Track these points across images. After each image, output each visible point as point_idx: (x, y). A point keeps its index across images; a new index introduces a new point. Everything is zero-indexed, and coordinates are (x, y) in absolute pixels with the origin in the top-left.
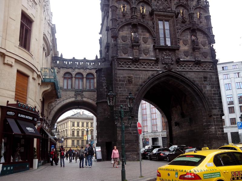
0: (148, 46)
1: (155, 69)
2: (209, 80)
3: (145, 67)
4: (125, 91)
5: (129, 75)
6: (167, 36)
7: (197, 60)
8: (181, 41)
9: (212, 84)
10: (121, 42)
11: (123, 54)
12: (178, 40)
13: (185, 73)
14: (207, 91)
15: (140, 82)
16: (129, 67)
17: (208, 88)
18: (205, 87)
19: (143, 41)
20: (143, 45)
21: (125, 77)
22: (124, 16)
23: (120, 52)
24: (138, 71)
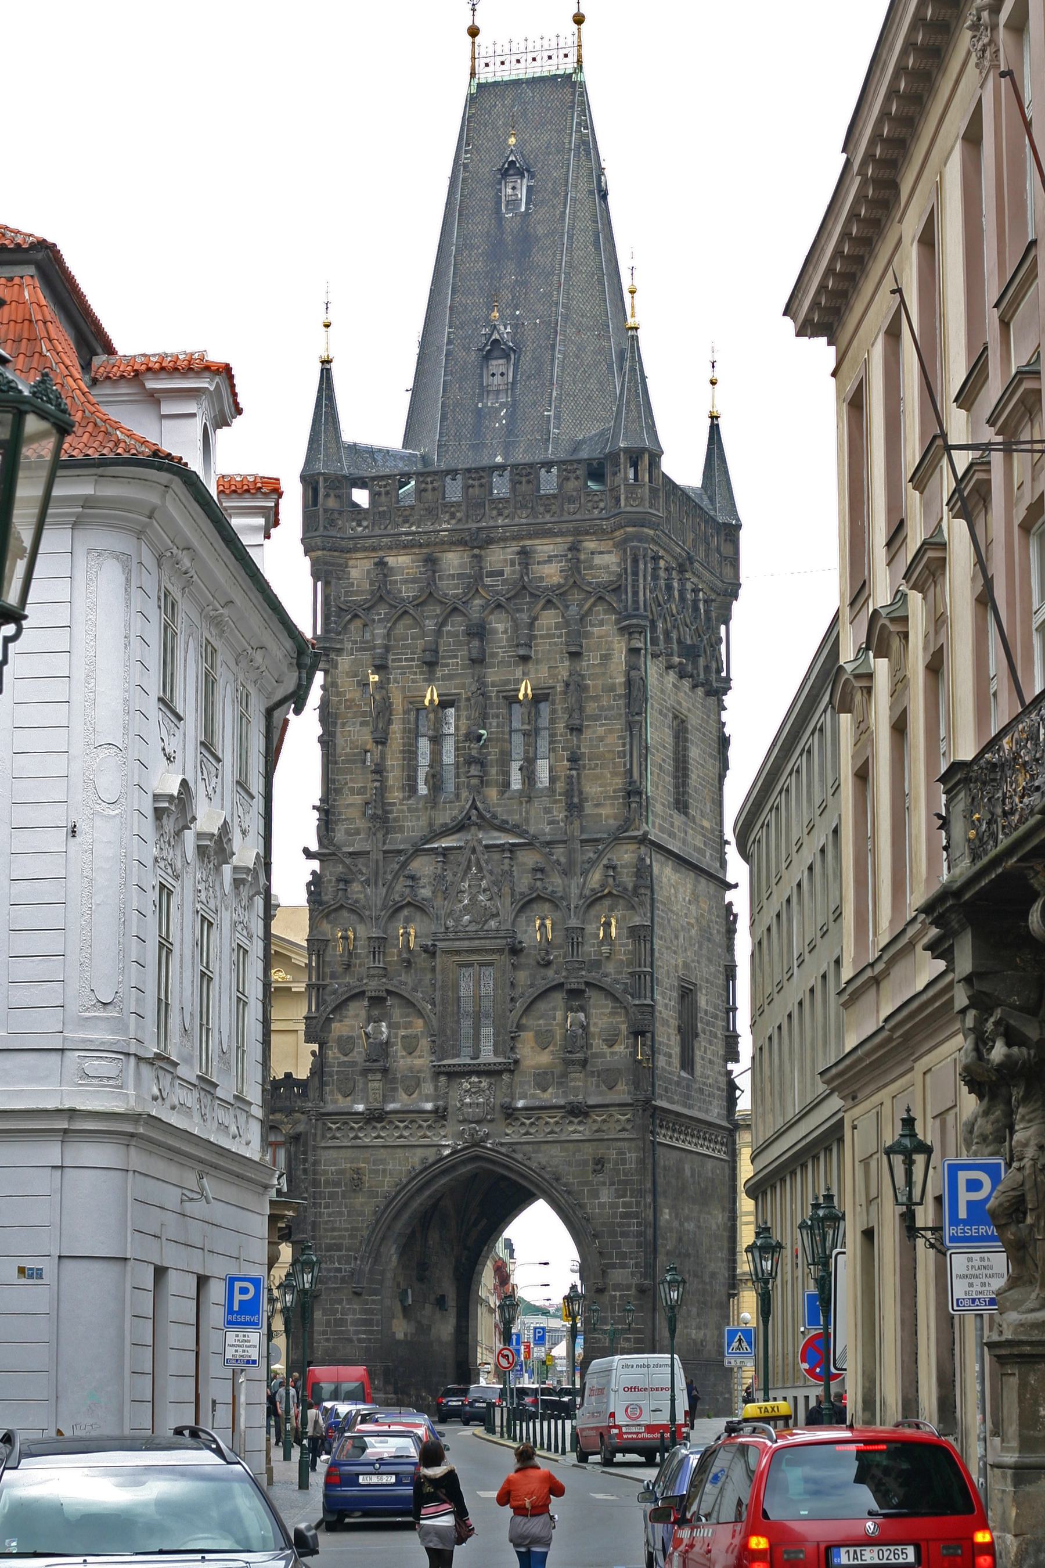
0: (418, 1062)
1: (436, 1140)
2: (611, 1170)
3: (406, 1133)
4: (341, 1213)
5: (355, 1165)
8: (528, 1036)
9: (620, 1182)
10: (338, 1058)
11: (340, 1097)
12: (512, 1038)
14: (602, 1206)
15: (387, 1185)
16: (356, 1137)
17: (606, 1196)
18: (595, 1194)
19: (404, 1048)
21: (341, 1172)
22: (348, 966)
23: (332, 1091)
24: (382, 1150)
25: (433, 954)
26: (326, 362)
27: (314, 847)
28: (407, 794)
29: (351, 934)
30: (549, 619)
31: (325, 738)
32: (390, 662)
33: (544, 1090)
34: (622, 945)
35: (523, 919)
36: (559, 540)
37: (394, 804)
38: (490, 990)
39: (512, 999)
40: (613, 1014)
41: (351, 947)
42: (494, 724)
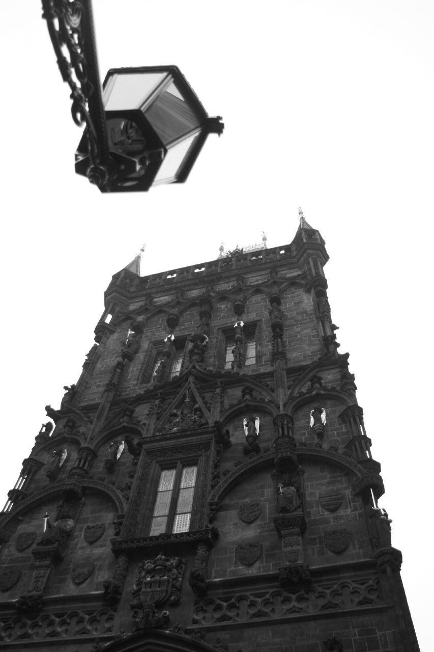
1: (95, 634)
6: (179, 510)
7: (285, 569)
13: (224, 636)
19: (86, 537)
20: (80, 551)
25: (139, 455)
26: (138, 258)
27: (57, 407)
28: (140, 381)
29: (65, 456)
30: (258, 298)
31: (88, 361)
32: (144, 331)
33: (250, 565)
34: (336, 430)
35: (230, 428)
36: (263, 273)
37: (128, 387)
38: (193, 483)
39: (216, 477)
40: (329, 483)
41: (61, 464)
42: (215, 341)
